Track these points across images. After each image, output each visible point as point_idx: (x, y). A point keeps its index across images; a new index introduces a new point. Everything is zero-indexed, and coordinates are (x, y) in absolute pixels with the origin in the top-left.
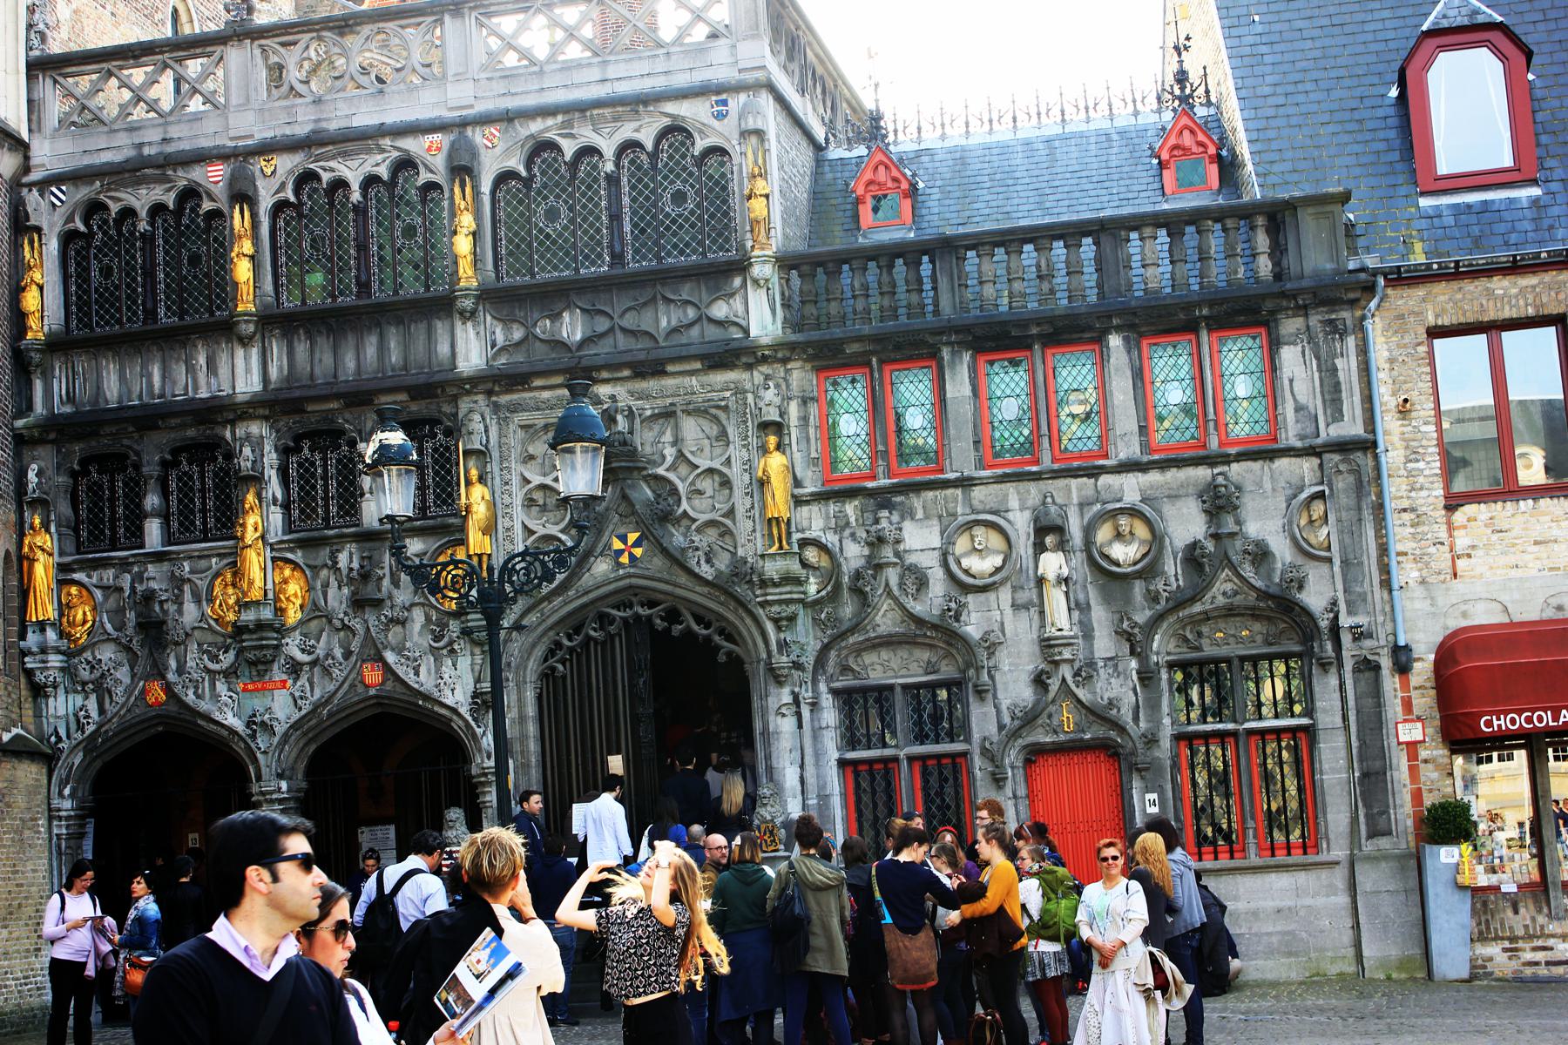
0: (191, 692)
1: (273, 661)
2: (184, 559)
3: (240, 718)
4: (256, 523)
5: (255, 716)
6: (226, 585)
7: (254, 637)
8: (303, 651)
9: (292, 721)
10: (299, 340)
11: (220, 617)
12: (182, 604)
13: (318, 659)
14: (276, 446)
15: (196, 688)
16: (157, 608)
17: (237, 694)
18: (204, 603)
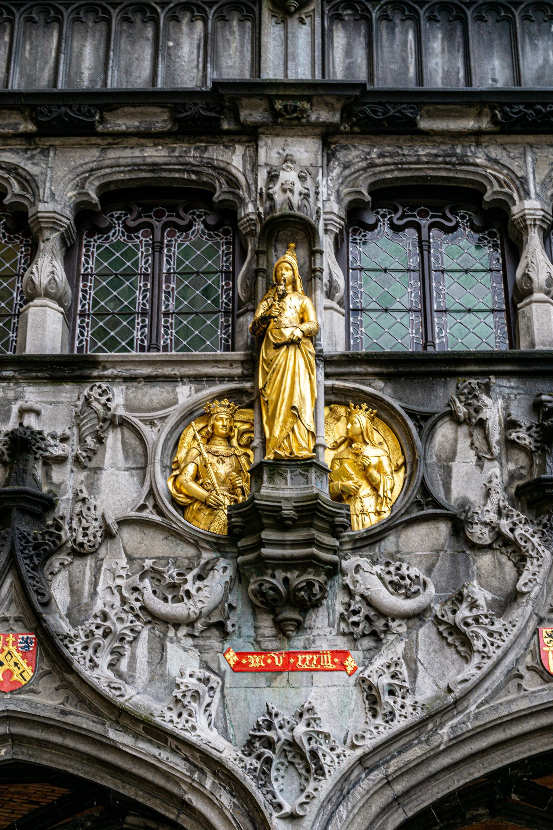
0: (103, 660)
1: (317, 605)
2: (113, 379)
3: (225, 733)
4: (303, 311)
5: (270, 726)
6: (209, 439)
7: (290, 537)
8: (395, 587)
9: (368, 744)
10: (392, 31)
11: (194, 499)
12: (98, 470)
13: (427, 609)
14: (338, 191)
15: (117, 653)
16: (39, 472)
17: (221, 675)
18: (158, 467)
